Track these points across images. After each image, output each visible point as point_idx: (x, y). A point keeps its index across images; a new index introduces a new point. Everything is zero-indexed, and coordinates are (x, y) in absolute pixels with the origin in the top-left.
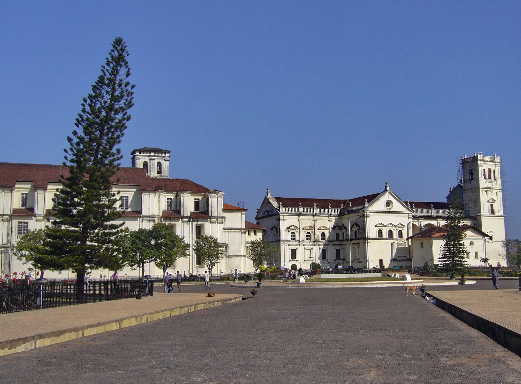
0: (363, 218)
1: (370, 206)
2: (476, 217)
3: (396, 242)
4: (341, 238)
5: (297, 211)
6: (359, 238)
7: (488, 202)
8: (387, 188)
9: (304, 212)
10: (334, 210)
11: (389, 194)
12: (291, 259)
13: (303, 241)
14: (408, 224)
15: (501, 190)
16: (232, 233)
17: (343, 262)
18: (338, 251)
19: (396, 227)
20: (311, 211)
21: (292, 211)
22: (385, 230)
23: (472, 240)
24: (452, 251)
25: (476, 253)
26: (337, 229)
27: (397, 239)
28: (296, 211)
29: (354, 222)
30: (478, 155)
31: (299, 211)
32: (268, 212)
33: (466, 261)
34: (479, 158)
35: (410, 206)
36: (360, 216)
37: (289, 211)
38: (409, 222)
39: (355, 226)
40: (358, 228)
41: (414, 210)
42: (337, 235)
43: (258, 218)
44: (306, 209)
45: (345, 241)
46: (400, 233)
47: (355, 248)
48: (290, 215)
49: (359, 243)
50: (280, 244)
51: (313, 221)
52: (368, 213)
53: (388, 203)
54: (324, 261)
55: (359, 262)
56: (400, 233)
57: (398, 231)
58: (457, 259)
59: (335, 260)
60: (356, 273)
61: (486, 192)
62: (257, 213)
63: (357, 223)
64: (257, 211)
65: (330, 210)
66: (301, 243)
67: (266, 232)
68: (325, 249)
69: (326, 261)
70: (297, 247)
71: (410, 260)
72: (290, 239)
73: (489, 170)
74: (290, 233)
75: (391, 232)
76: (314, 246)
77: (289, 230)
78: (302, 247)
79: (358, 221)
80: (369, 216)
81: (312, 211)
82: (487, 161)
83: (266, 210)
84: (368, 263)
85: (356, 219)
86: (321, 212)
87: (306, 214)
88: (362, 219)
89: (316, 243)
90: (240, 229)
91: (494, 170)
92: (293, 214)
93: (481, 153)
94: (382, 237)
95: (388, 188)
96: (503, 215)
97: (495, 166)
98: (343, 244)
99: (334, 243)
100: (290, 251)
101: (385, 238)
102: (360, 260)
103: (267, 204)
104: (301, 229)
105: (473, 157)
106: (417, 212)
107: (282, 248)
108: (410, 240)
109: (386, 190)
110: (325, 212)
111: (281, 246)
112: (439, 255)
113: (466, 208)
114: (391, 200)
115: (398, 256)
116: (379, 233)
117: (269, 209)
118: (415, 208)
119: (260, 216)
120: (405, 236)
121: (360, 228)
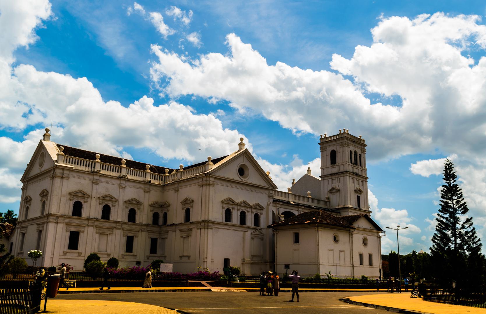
4: (161, 222)
12: (66, 249)
19: (251, 207)
22: (236, 210)
25: (370, 256)
38: (269, 203)
46: (257, 218)
53: (242, 171)
57: (253, 215)
59: (148, 257)
61: (353, 179)
73: (356, 153)
91: (360, 155)
99: (149, 228)
100: (68, 234)
105: (338, 135)
114: (245, 165)
120: (263, 223)
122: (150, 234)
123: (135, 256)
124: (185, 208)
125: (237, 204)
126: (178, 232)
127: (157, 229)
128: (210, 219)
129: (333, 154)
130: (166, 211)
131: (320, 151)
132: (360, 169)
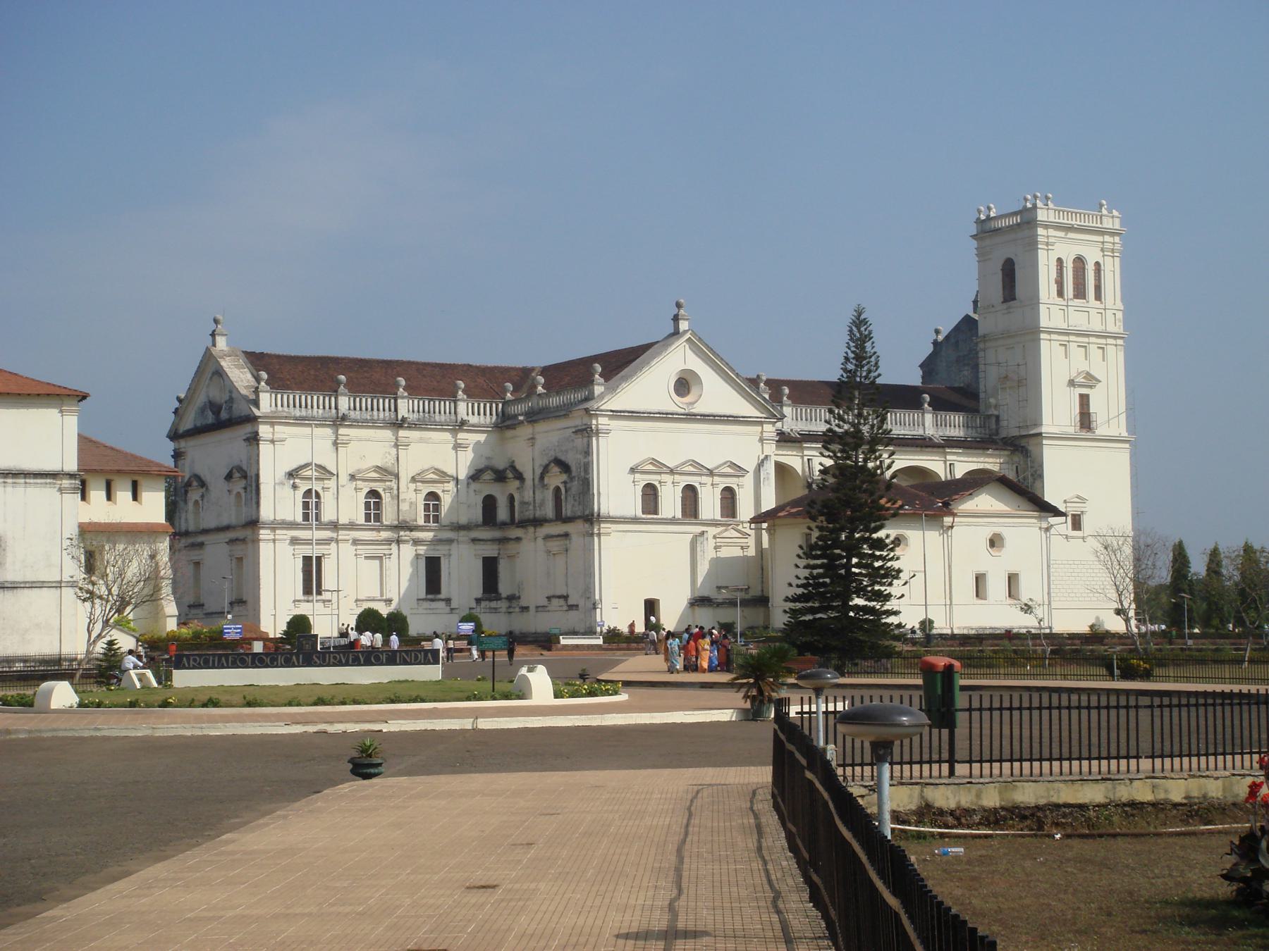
0: (585, 440)
1: (612, 390)
2: (1023, 442)
3: (712, 531)
4: (502, 514)
5: (330, 408)
6: (569, 514)
7: (1072, 383)
8: (680, 322)
9: (358, 413)
10: (476, 405)
11: (687, 346)
12: (300, 595)
13: (352, 526)
14: (760, 465)
15: (1120, 342)
16: (20, 490)
17: (510, 607)
18: (490, 568)
20: (384, 410)
21: (309, 407)
22: (669, 484)
23: (997, 530)
24: (843, 572)
25: (1012, 579)
26: (485, 482)
27: (714, 520)
28: (324, 408)
29: (552, 454)
30: (1039, 204)
31: (336, 408)
32: (215, 407)
33: (896, 613)
34: (1042, 215)
35: (767, 396)
36: (574, 430)
37: (294, 406)
38: (762, 457)
39: (555, 469)
40: (564, 477)
41: (787, 410)
42: (489, 504)
43: (181, 430)
44: (366, 401)
45: (518, 527)
47: (554, 554)
48: (301, 421)
49: (566, 535)
50: (259, 535)
51: (394, 451)
52: (602, 420)
53: (684, 385)
54: (434, 605)
55: (565, 608)
56: (729, 497)
57: (718, 491)
58: (860, 602)
59: (478, 601)
60: (328, 665)
61: (1065, 345)
62: (176, 412)
63: (563, 458)
64: (177, 404)
65: (462, 407)
66: (343, 534)
67: (207, 489)
68: (439, 558)
69: (442, 605)
70: (327, 547)
71: (762, 601)
72: (299, 519)
73: (1080, 261)
74: (300, 493)
75: (690, 495)
76: (394, 546)
77: (296, 480)
78: (347, 550)
79: (567, 451)
80: (608, 432)
81: (390, 410)
82: (1070, 229)
83: (210, 402)
84: (598, 611)
85: (558, 442)
86: (424, 411)
87: (366, 421)
88: (579, 442)
89: (402, 533)
90: (54, 475)
91: (1097, 264)
92: (313, 418)
93: (1050, 195)
94: (656, 512)
95: (684, 325)
96: (1126, 435)
97: (1102, 250)
98: (511, 539)
100: (299, 563)
101: (670, 517)
102: (571, 602)
103: (211, 378)
104: (344, 478)
106: (794, 419)
107: (265, 550)
108: (765, 525)
109: (676, 333)
110: (440, 413)
111: (261, 544)
112: (790, 585)
113: (989, 406)
115: (719, 588)
116: (644, 495)
117: (219, 396)
118: (790, 402)
119: (187, 424)
120: (746, 510)
121: (572, 479)
122: (478, 547)
123: (448, 601)
124: (552, 488)
125: (672, 472)
126: (540, 541)
127: (497, 534)
128: (604, 511)
129: (1008, 270)
130: (511, 492)
131: (977, 259)
132: (1093, 312)
